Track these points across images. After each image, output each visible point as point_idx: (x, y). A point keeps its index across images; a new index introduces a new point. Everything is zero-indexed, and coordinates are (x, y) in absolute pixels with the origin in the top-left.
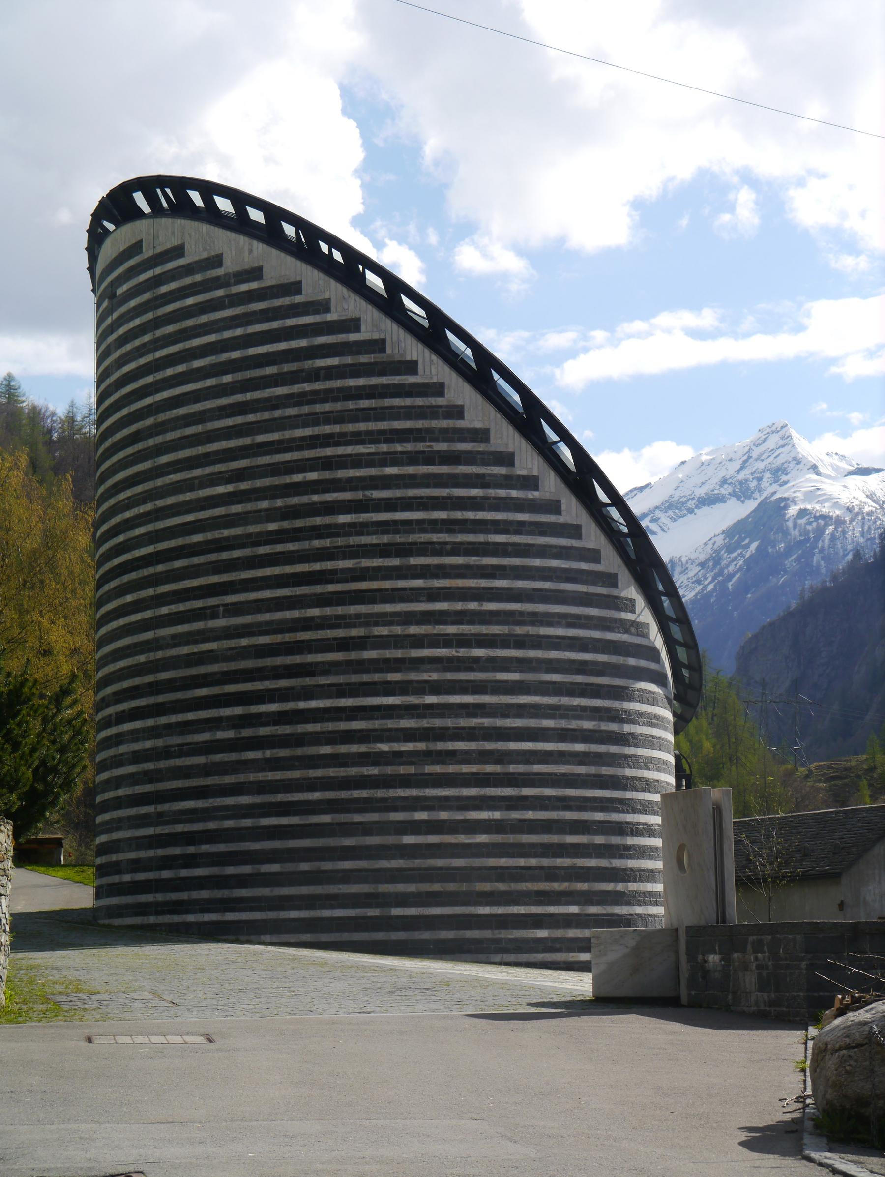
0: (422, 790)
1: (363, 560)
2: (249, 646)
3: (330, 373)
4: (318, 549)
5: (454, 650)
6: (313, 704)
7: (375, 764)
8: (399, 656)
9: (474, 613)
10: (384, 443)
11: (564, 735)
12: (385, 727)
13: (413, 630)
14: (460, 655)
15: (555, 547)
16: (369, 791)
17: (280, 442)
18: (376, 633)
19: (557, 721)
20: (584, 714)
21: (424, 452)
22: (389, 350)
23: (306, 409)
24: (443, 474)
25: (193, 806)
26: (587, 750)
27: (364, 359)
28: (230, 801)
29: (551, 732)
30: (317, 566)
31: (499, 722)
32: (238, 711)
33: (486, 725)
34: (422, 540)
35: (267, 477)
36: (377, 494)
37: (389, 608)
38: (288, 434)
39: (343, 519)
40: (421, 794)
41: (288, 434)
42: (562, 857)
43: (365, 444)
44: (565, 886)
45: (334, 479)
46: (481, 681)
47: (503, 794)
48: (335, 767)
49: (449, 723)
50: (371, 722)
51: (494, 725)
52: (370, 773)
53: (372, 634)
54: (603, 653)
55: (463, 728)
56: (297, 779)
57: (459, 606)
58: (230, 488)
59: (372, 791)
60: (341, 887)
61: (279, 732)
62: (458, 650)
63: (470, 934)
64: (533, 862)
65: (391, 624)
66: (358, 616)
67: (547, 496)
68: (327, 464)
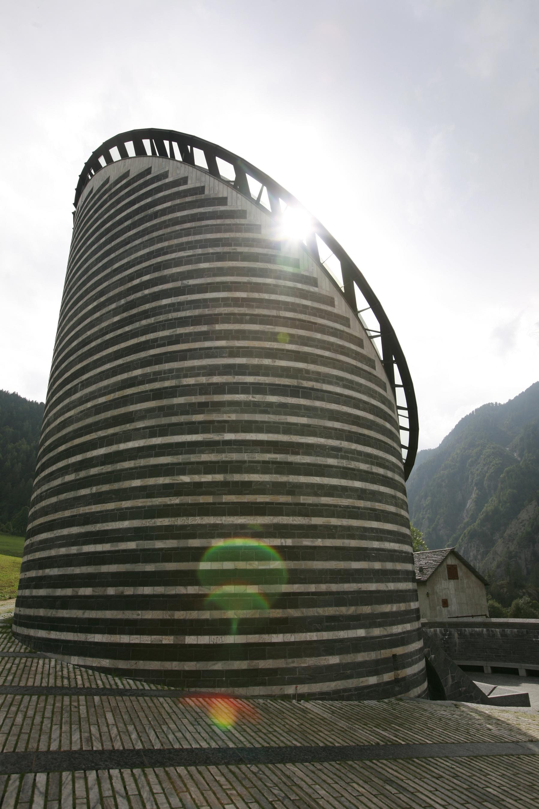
0: (219, 518)
1: (178, 329)
2: (92, 407)
3: (164, 212)
4: (145, 326)
5: (251, 396)
6: (131, 445)
7: (177, 494)
8: (203, 401)
9: (267, 367)
10: (200, 248)
11: (346, 473)
12: (188, 461)
13: (216, 379)
14: (255, 400)
15: (332, 328)
16: (170, 519)
17: (128, 263)
18: (185, 383)
19: (339, 460)
20: (360, 457)
21: (229, 253)
22: (207, 192)
23: (146, 238)
24: (244, 267)
25: (46, 537)
26: (364, 487)
27: (189, 199)
28: (65, 532)
29: (334, 469)
30: (143, 339)
31: (291, 458)
32: (79, 458)
33: (278, 460)
34: (226, 312)
35: (117, 288)
36: (191, 282)
37: (196, 363)
38: (133, 257)
39: (165, 302)
40: (218, 522)
41: (133, 257)
42: (349, 582)
43: (186, 250)
44: (351, 610)
45: (161, 277)
46: (274, 423)
47: (295, 522)
48: (143, 498)
49: (245, 457)
50: (176, 457)
51: (285, 460)
52: (172, 502)
53: (181, 384)
54: (370, 413)
55: (258, 462)
56: (113, 510)
57: (255, 361)
58: (95, 304)
59: (173, 519)
60: (140, 612)
61: (104, 471)
62: (254, 396)
63: (263, 664)
64: (323, 587)
65: (198, 375)
66: (171, 371)
67: (324, 292)
68: (158, 267)
